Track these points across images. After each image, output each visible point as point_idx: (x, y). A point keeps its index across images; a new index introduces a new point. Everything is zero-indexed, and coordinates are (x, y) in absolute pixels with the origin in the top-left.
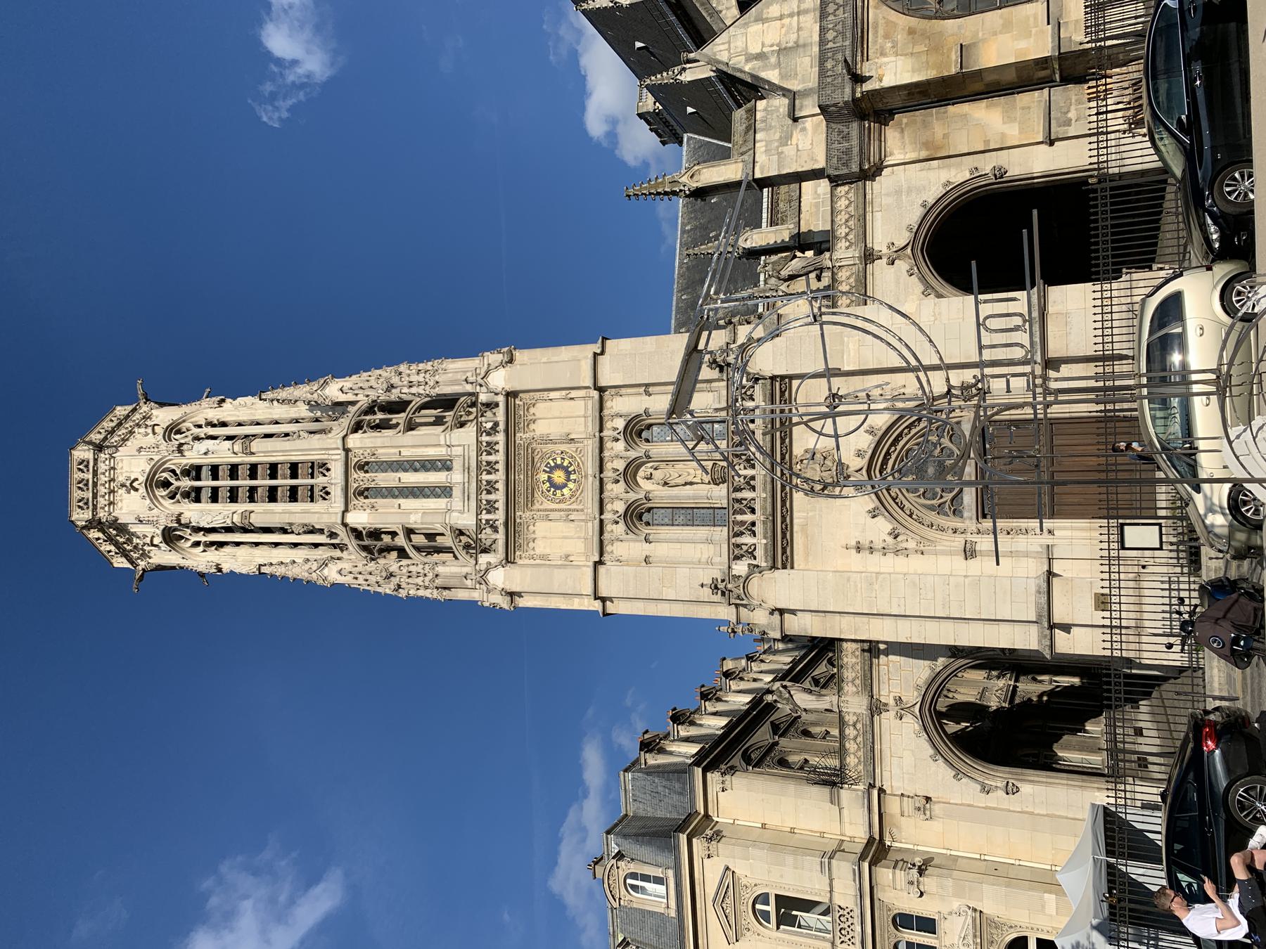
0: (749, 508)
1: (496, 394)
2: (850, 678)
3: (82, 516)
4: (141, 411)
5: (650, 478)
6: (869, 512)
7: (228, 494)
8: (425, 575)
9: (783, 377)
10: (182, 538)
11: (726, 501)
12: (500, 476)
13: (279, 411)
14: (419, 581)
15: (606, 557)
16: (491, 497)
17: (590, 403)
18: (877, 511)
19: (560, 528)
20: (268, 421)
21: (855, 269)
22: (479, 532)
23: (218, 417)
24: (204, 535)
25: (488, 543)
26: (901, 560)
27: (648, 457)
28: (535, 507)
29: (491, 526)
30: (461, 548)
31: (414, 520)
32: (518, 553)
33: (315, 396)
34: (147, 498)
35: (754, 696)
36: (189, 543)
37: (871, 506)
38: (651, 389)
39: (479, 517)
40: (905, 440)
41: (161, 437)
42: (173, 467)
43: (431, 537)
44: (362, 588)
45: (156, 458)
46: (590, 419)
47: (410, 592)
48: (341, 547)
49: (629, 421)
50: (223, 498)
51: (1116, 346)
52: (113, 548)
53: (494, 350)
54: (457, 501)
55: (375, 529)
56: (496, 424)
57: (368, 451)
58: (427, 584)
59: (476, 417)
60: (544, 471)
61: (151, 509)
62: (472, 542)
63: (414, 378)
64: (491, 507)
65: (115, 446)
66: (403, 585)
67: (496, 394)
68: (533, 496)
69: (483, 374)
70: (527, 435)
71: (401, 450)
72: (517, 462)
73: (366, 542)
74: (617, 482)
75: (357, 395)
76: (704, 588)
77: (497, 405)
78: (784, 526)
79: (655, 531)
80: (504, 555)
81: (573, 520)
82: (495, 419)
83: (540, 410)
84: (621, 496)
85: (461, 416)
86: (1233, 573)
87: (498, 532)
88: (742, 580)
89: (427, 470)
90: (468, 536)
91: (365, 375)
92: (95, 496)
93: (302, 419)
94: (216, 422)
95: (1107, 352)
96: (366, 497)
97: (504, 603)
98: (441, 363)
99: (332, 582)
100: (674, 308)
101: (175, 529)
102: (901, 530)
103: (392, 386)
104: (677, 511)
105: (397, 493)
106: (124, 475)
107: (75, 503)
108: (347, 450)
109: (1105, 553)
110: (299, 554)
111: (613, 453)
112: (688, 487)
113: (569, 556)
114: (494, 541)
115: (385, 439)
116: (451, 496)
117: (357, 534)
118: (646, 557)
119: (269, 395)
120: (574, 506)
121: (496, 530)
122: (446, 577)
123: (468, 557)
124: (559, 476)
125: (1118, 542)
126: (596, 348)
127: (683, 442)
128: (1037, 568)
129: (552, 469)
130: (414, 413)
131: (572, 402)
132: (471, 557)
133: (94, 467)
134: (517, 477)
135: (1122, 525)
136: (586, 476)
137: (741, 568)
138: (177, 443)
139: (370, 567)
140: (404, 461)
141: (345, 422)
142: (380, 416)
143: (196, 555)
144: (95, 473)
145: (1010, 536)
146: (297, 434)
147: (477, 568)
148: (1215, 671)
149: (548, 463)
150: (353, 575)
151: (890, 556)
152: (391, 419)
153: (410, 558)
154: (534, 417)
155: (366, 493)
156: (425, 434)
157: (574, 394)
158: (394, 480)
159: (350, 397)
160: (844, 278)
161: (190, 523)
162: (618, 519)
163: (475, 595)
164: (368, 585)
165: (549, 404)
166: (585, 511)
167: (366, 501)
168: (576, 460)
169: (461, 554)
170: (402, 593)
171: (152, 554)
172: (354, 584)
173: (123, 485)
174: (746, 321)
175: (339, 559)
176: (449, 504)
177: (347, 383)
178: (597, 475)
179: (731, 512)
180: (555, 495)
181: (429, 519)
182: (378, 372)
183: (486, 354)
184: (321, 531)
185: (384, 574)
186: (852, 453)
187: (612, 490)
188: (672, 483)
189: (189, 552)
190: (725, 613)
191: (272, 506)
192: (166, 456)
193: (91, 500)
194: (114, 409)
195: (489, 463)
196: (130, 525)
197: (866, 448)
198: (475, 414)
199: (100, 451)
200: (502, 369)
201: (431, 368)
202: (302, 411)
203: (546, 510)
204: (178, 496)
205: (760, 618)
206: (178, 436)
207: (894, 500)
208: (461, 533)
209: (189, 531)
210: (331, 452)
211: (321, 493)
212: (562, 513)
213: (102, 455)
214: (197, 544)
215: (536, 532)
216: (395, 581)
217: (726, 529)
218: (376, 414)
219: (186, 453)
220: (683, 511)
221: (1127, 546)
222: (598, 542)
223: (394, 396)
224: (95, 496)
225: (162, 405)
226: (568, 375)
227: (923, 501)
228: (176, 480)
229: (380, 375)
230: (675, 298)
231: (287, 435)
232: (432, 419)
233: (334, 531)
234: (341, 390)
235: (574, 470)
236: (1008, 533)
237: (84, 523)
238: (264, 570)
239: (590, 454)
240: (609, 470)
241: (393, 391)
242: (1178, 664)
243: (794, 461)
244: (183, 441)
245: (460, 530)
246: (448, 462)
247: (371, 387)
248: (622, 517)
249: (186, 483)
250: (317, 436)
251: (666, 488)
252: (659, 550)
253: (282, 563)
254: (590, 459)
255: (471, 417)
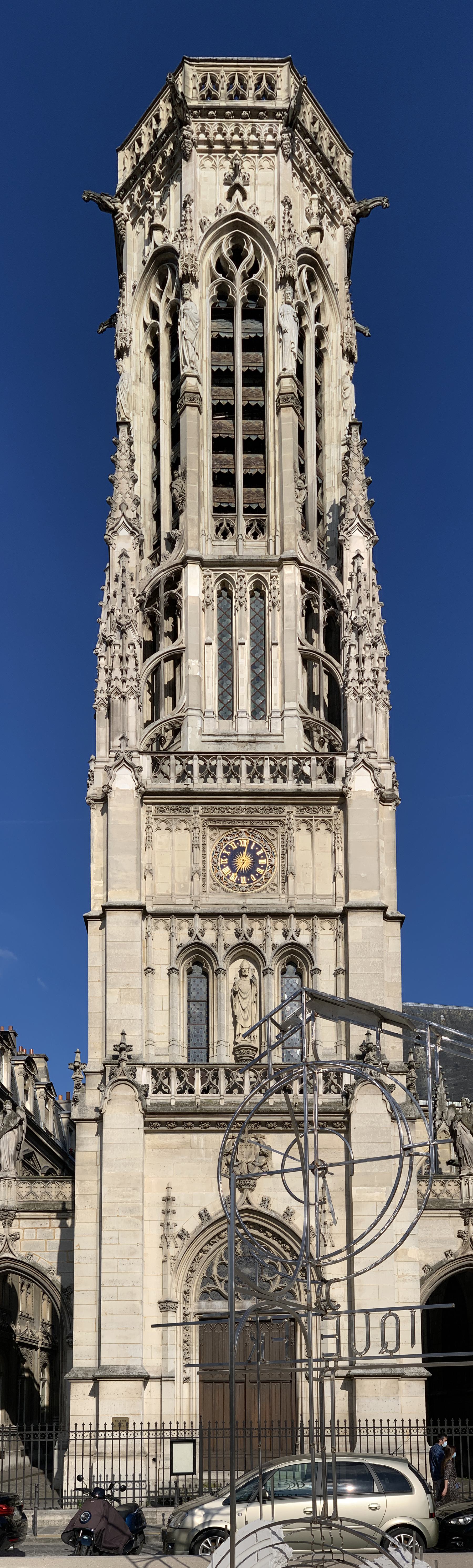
0: (209, 1088)
1: (344, 780)
2: (34, 1190)
3: (191, 86)
4: (343, 206)
5: (242, 974)
6: (205, 1211)
7: (223, 369)
8: (124, 681)
9: (348, 1124)
10: (163, 285)
11: (215, 1062)
12: (245, 784)
13: (334, 453)
14: (117, 673)
15: (151, 921)
16: (220, 773)
17: (329, 901)
18: (206, 1218)
19: (184, 864)
20: (322, 438)
21: (457, 1198)
22: (178, 755)
23: (329, 350)
24: (168, 325)
25: (165, 768)
26: (156, 1241)
27: (265, 973)
28: (207, 830)
29: (184, 773)
30: (158, 731)
31: (191, 665)
32: (153, 808)
33: (352, 515)
34: (218, 218)
35: (9, 1090)
36: (155, 299)
37: (211, 1213)
38: (341, 976)
39: (195, 756)
40: (279, 1246)
41: (305, 244)
42: (262, 268)
43: (171, 690)
44: (105, 588)
45: (275, 235)
46: (310, 902)
47: (102, 659)
48: (156, 558)
49: (307, 950)
50: (219, 359)
51: (364, 1439)
52: (145, 149)
53: (397, 777)
54: (215, 725)
55: (180, 608)
56: (308, 779)
57: (279, 597)
58: (113, 683)
59: (316, 753)
60: (251, 842)
61: (203, 224)
62: (165, 747)
63: (368, 665)
64: (208, 772)
65: (293, 153)
66: (111, 650)
67: (344, 780)
68: (221, 828)
69: (369, 761)
70: (293, 821)
71: (279, 647)
72: (262, 807)
73: (162, 594)
74: (237, 935)
75: (351, 579)
76: (121, 1036)
77: (331, 780)
78: (190, 1124)
79: (181, 980)
80: (151, 790)
81: (192, 879)
82: (314, 778)
83: (323, 837)
84: (221, 940)
85: (319, 732)
86: (150, 1533)
87: (178, 781)
88: (131, 1078)
89: (253, 684)
90: (172, 742)
91: (375, 592)
92: (221, 112)
93: (322, 494)
94: (322, 347)
95: (358, 1431)
96: (220, 595)
97: (94, 790)
98: (385, 704)
99: (111, 541)
100: (431, 1006)
101: (174, 273)
102: (187, 1242)
103: (359, 633)
104: (204, 1006)
105: (225, 640)
106: (251, 172)
107: (210, 69)
108: (279, 565)
109: (167, 1426)
110: (144, 489)
111: (270, 930)
112: (231, 1019)
113: (152, 874)
114: (167, 777)
115: (293, 623)
116: (221, 717)
117: (174, 580)
118: (153, 970)
119: (356, 440)
120: (209, 881)
121: (180, 778)
122: (123, 710)
123: (147, 741)
124: (244, 861)
125: (178, 1437)
126: (392, 911)
127: (281, 1007)
128: (152, 1366)
129: (252, 853)
130: (325, 665)
131: (331, 879)
132: (148, 746)
133: (263, 109)
134: (243, 807)
135: (194, 1442)
136: (244, 896)
137: (144, 1077)
138: (296, 275)
139: (132, 602)
140: (265, 650)
141: (316, 562)
142: (322, 614)
143: (139, 311)
144: (255, 113)
145: (182, 1343)
146: (303, 485)
147: (135, 754)
148: (60, 1518)
149: (260, 848)
150: (120, 574)
151: (160, 1231)
152: (318, 632)
153: (144, 660)
154: (314, 829)
155: (225, 593)
156: (297, 680)
157: (340, 881)
158: (241, 636)
159: (348, 569)
160: (448, 1188)
161: (185, 300)
162: (194, 936)
163: (102, 752)
164: (109, 598)
165: (330, 849)
166: (204, 896)
167: (215, 594)
168: (263, 883)
169: (150, 733)
170: (100, 649)
171: (138, 227)
172: (110, 577)
173: (236, 169)
174: (411, 1085)
175: (141, 552)
176: (211, 715)
177: (366, 565)
178: (245, 910)
179: (203, 1067)
180: (222, 857)
181: (193, 686)
182: (378, 612)
183: (393, 766)
184: (175, 525)
185: (123, 621)
186: (266, 1195)
187: (228, 929)
188: (236, 1001)
189: (143, 298)
190: (95, 1059)
191: (208, 444)
192: (277, 253)
193: (215, 103)
194: (348, 152)
195: (261, 769)
196: (178, 184)
197: (271, 1208)
198: (320, 751)
199: (286, 125)
200: (374, 788)
201: (379, 689)
202: (334, 494)
203: (204, 844)
204: (221, 277)
205: (92, 1097)
206: (304, 275)
207: (218, 1235)
208: (177, 731)
209: (172, 298)
210: (278, 539)
211: (225, 524)
212: (201, 866)
213: (280, 128)
214: (155, 314)
215: (178, 832)
216: (115, 637)
217: (185, 1061)
218: (325, 608)
219: (280, 292)
220: (204, 1013)
221: (174, 1445)
222: (169, 911)
223: (348, 636)
224: (221, 112)
225: (351, 245)
226: (363, 875)
227: (216, 1262)
228: (243, 273)
229: (374, 615)
230: (441, 1007)
231: (302, 468)
232: (316, 690)
233: (177, 544)
234: (358, 556)
235: (251, 881)
236: (185, 1342)
237: (180, 89)
238: (123, 430)
239: (270, 901)
240: (250, 924)
241: (354, 635)
242: (65, 1488)
243: (259, 1135)
244: (297, 285)
245: (179, 730)
246: (262, 714)
247: (360, 601)
248: (197, 941)
249: (239, 292)
250: (299, 518)
251: (230, 994)
252: (160, 983)
253: (133, 461)
254: (264, 901)
255: (317, 746)
